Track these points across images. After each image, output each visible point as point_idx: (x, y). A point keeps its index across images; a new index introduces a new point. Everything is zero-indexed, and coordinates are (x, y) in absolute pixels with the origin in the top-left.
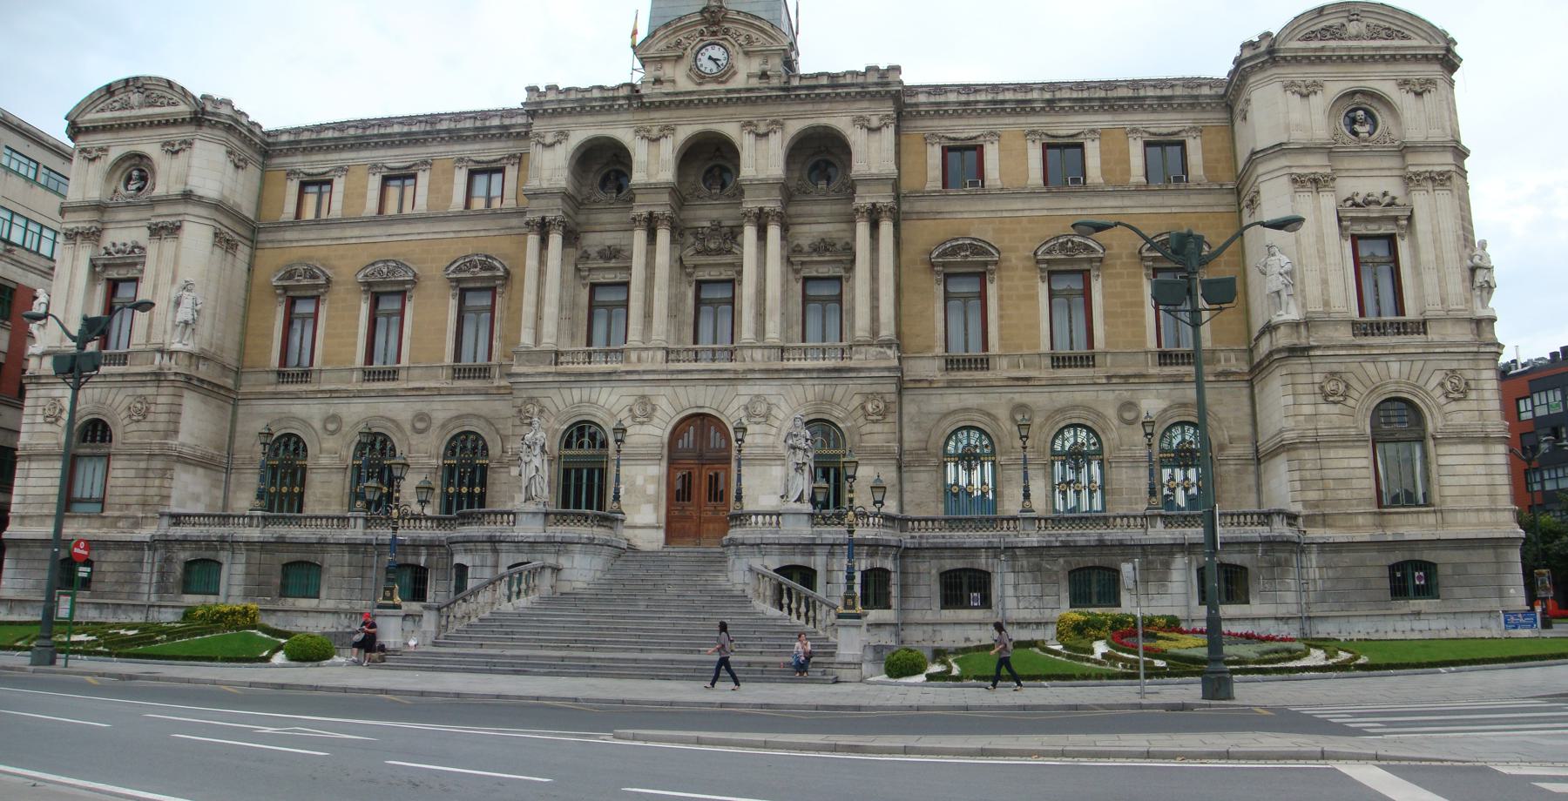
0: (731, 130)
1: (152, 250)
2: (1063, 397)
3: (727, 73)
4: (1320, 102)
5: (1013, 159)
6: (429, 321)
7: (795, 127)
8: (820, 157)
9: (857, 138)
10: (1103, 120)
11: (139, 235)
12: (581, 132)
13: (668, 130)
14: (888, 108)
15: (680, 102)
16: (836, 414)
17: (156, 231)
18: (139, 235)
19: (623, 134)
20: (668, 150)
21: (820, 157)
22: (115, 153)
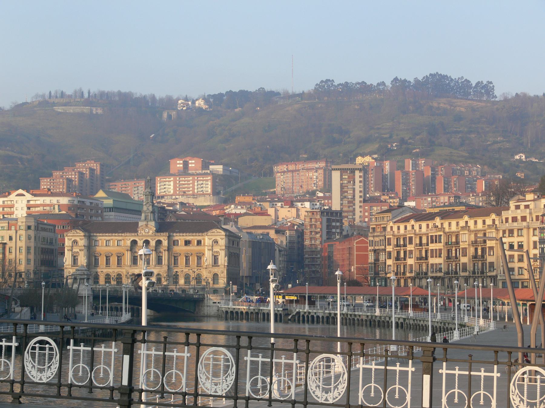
0: (149, 239)
1: (80, 252)
2: (187, 270)
3: (148, 232)
4: (211, 241)
5: (181, 242)
6: (114, 260)
7: (156, 239)
8: (159, 242)
9: (163, 241)
10: (192, 237)
11: (78, 251)
12: (132, 239)
13: (142, 239)
14: (167, 238)
15: (143, 236)
16: (161, 273)
17: (80, 250)
18: (78, 251)
19: (137, 239)
20: (142, 242)
21: (159, 242)
22: (73, 240)
